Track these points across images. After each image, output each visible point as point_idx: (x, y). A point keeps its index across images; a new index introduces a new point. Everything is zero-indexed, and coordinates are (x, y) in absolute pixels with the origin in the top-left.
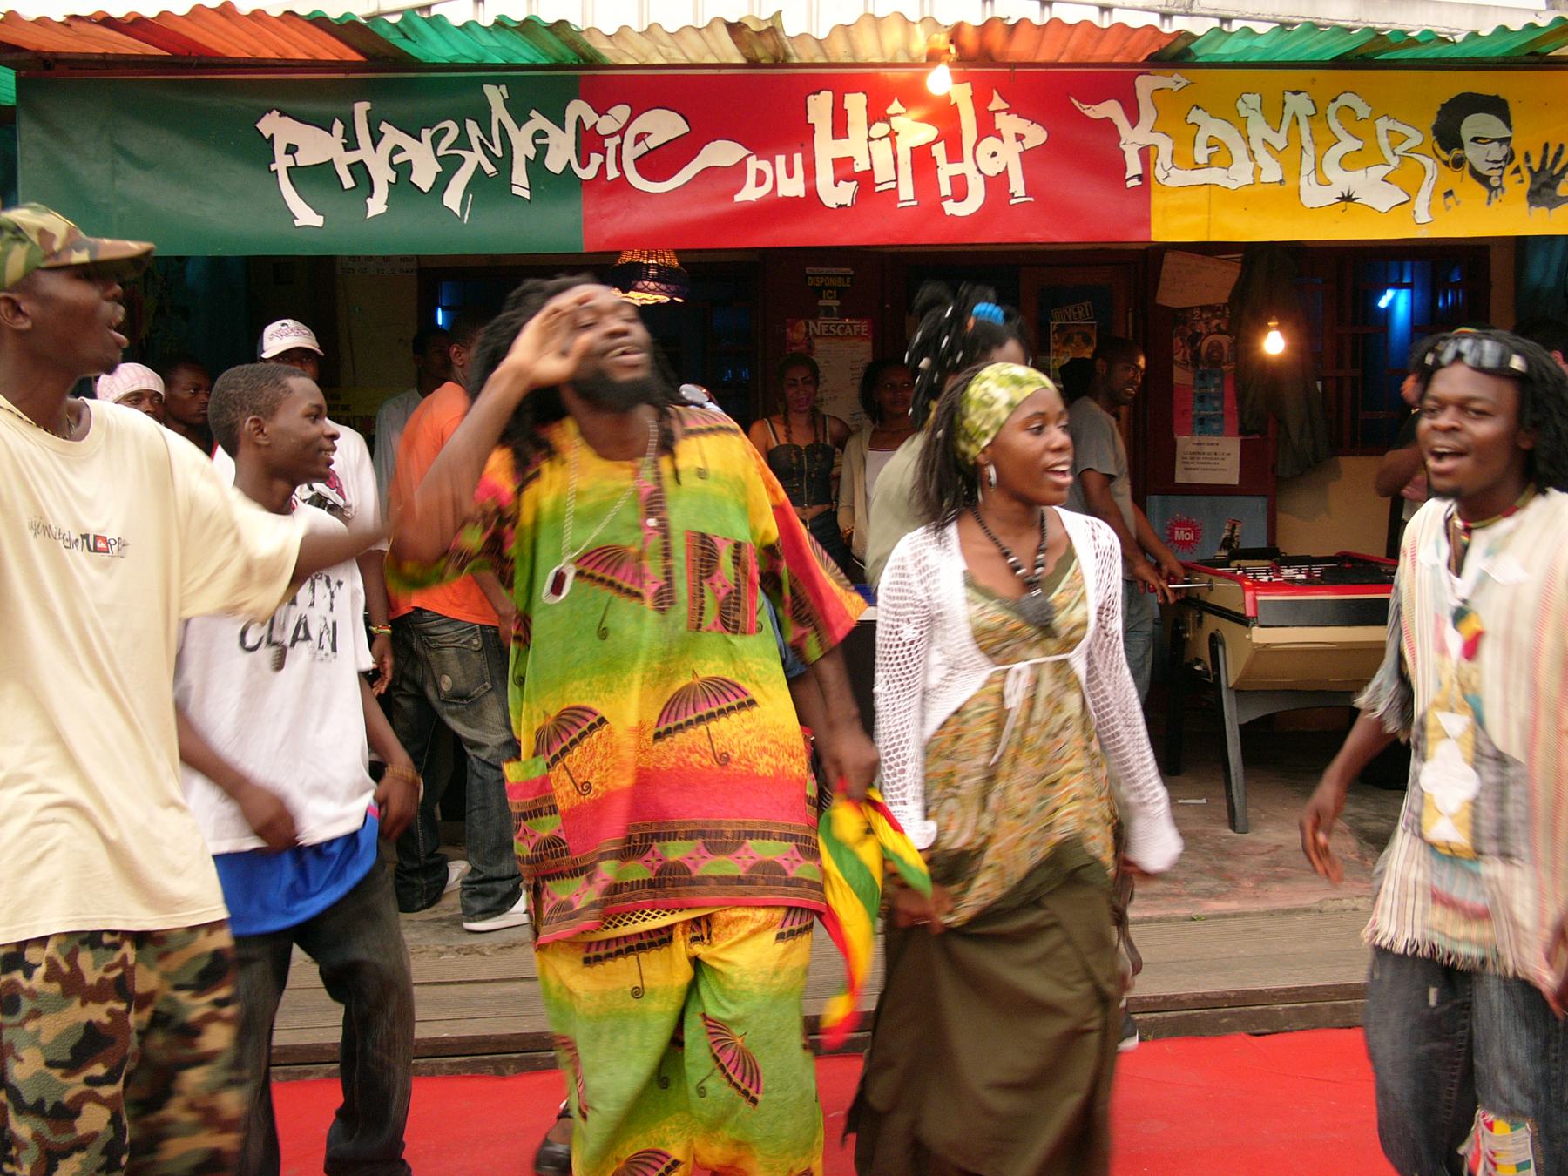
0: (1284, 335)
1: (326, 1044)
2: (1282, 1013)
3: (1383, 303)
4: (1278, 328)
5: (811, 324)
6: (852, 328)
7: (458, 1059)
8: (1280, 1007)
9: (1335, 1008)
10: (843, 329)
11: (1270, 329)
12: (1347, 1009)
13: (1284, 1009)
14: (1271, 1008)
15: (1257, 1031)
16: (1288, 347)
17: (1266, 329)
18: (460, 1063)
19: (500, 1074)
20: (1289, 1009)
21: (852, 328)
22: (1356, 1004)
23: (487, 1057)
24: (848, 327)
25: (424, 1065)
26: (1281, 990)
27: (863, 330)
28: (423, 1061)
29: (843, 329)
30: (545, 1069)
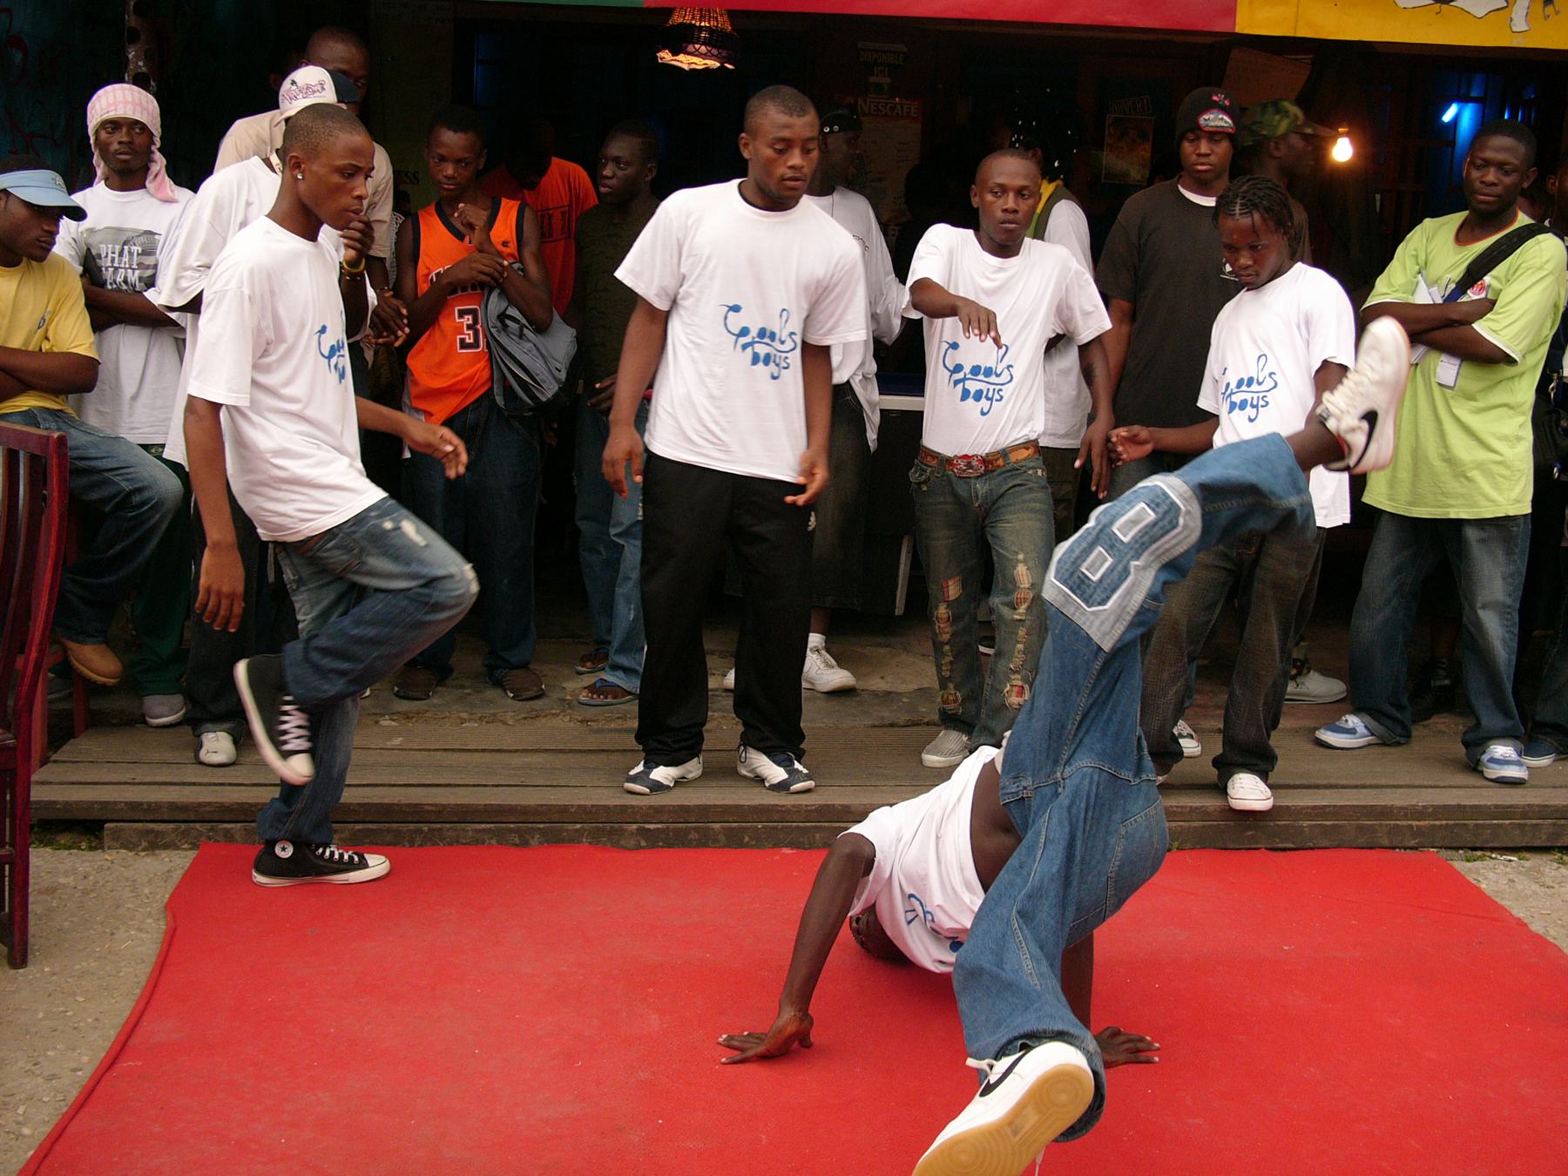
0: (1352, 142)
1: (351, 804)
2: (1306, 829)
3: (1447, 117)
4: (1347, 135)
5: (860, 101)
6: (902, 108)
7: (483, 826)
8: (1306, 823)
9: (1360, 828)
10: (892, 109)
11: (1342, 135)
12: (1372, 829)
13: (1310, 826)
14: (1296, 823)
15: (1280, 846)
16: (1356, 154)
17: (1334, 139)
18: (484, 830)
19: (525, 844)
20: (1314, 825)
21: (902, 108)
22: (1381, 825)
23: (512, 825)
24: (898, 106)
25: (448, 830)
26: (1308, 807)
27: (913, 111)
28: (448, 826)
29: (892, 109)
30: (572, 841)
